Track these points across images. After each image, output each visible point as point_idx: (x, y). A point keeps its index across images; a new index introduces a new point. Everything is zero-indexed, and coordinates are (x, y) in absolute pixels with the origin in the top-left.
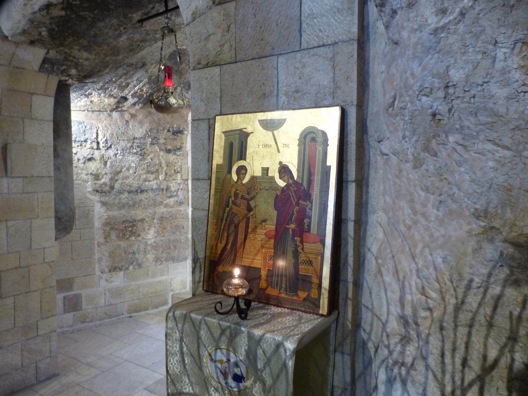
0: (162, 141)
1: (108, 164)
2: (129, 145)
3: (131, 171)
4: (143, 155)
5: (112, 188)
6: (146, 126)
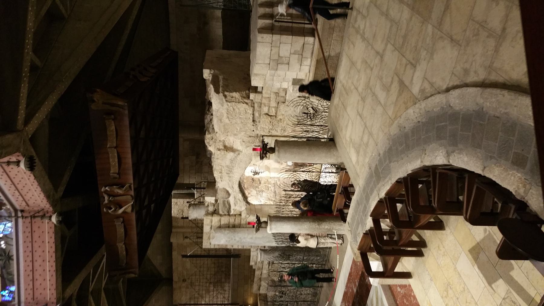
0: (257, 185)
1: (266, 202)
2: (259, 195)
3: (268, 195)
4: (263, 191)
5: (274, 201)
6: (252, 189)
